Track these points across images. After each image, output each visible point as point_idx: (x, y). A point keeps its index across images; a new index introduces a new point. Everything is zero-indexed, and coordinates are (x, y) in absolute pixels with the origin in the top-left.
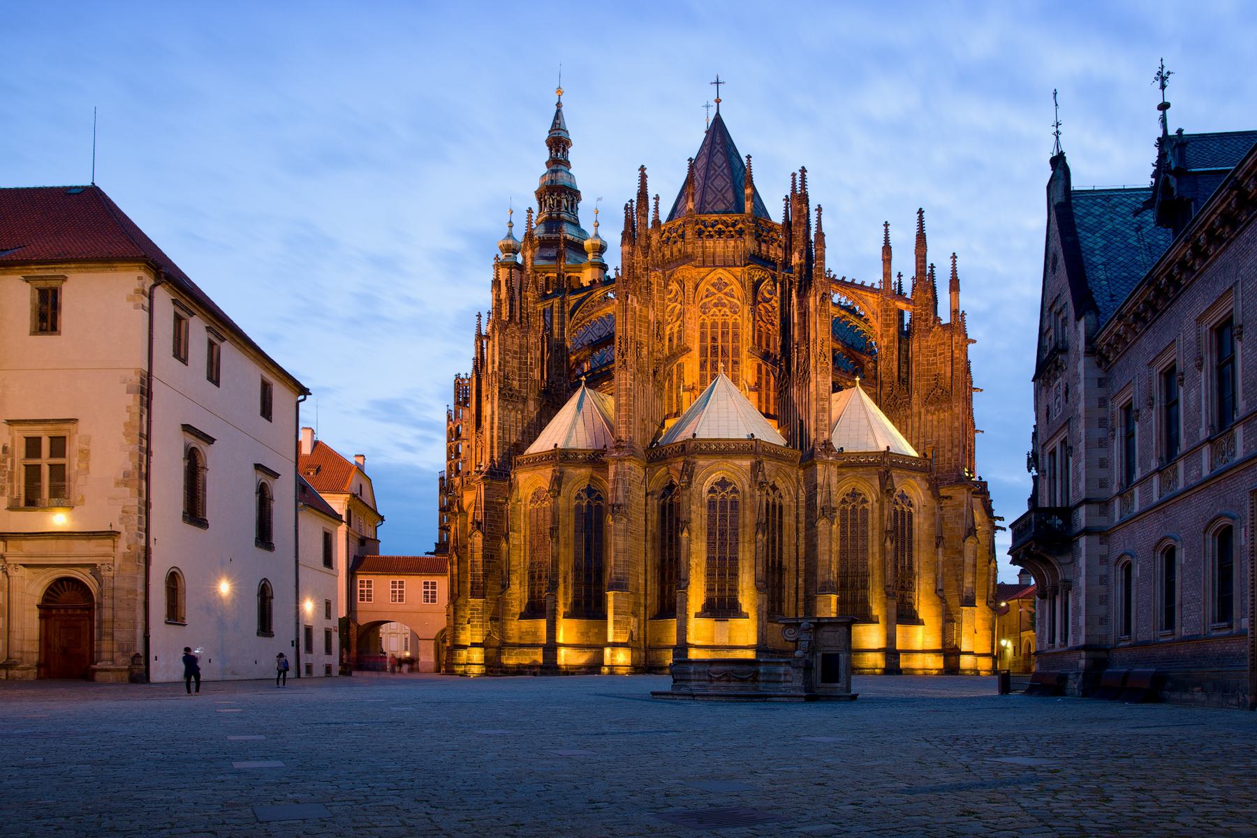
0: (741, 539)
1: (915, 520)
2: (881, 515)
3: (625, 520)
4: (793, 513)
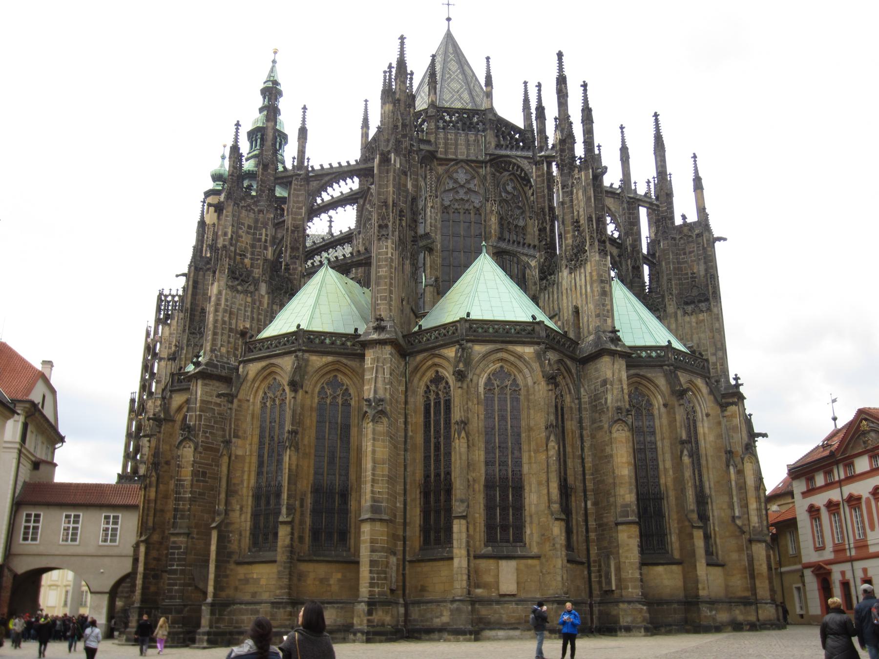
1: (700, 430)
2: (672, 421)
3: (385, 420)
4: (576, 416)
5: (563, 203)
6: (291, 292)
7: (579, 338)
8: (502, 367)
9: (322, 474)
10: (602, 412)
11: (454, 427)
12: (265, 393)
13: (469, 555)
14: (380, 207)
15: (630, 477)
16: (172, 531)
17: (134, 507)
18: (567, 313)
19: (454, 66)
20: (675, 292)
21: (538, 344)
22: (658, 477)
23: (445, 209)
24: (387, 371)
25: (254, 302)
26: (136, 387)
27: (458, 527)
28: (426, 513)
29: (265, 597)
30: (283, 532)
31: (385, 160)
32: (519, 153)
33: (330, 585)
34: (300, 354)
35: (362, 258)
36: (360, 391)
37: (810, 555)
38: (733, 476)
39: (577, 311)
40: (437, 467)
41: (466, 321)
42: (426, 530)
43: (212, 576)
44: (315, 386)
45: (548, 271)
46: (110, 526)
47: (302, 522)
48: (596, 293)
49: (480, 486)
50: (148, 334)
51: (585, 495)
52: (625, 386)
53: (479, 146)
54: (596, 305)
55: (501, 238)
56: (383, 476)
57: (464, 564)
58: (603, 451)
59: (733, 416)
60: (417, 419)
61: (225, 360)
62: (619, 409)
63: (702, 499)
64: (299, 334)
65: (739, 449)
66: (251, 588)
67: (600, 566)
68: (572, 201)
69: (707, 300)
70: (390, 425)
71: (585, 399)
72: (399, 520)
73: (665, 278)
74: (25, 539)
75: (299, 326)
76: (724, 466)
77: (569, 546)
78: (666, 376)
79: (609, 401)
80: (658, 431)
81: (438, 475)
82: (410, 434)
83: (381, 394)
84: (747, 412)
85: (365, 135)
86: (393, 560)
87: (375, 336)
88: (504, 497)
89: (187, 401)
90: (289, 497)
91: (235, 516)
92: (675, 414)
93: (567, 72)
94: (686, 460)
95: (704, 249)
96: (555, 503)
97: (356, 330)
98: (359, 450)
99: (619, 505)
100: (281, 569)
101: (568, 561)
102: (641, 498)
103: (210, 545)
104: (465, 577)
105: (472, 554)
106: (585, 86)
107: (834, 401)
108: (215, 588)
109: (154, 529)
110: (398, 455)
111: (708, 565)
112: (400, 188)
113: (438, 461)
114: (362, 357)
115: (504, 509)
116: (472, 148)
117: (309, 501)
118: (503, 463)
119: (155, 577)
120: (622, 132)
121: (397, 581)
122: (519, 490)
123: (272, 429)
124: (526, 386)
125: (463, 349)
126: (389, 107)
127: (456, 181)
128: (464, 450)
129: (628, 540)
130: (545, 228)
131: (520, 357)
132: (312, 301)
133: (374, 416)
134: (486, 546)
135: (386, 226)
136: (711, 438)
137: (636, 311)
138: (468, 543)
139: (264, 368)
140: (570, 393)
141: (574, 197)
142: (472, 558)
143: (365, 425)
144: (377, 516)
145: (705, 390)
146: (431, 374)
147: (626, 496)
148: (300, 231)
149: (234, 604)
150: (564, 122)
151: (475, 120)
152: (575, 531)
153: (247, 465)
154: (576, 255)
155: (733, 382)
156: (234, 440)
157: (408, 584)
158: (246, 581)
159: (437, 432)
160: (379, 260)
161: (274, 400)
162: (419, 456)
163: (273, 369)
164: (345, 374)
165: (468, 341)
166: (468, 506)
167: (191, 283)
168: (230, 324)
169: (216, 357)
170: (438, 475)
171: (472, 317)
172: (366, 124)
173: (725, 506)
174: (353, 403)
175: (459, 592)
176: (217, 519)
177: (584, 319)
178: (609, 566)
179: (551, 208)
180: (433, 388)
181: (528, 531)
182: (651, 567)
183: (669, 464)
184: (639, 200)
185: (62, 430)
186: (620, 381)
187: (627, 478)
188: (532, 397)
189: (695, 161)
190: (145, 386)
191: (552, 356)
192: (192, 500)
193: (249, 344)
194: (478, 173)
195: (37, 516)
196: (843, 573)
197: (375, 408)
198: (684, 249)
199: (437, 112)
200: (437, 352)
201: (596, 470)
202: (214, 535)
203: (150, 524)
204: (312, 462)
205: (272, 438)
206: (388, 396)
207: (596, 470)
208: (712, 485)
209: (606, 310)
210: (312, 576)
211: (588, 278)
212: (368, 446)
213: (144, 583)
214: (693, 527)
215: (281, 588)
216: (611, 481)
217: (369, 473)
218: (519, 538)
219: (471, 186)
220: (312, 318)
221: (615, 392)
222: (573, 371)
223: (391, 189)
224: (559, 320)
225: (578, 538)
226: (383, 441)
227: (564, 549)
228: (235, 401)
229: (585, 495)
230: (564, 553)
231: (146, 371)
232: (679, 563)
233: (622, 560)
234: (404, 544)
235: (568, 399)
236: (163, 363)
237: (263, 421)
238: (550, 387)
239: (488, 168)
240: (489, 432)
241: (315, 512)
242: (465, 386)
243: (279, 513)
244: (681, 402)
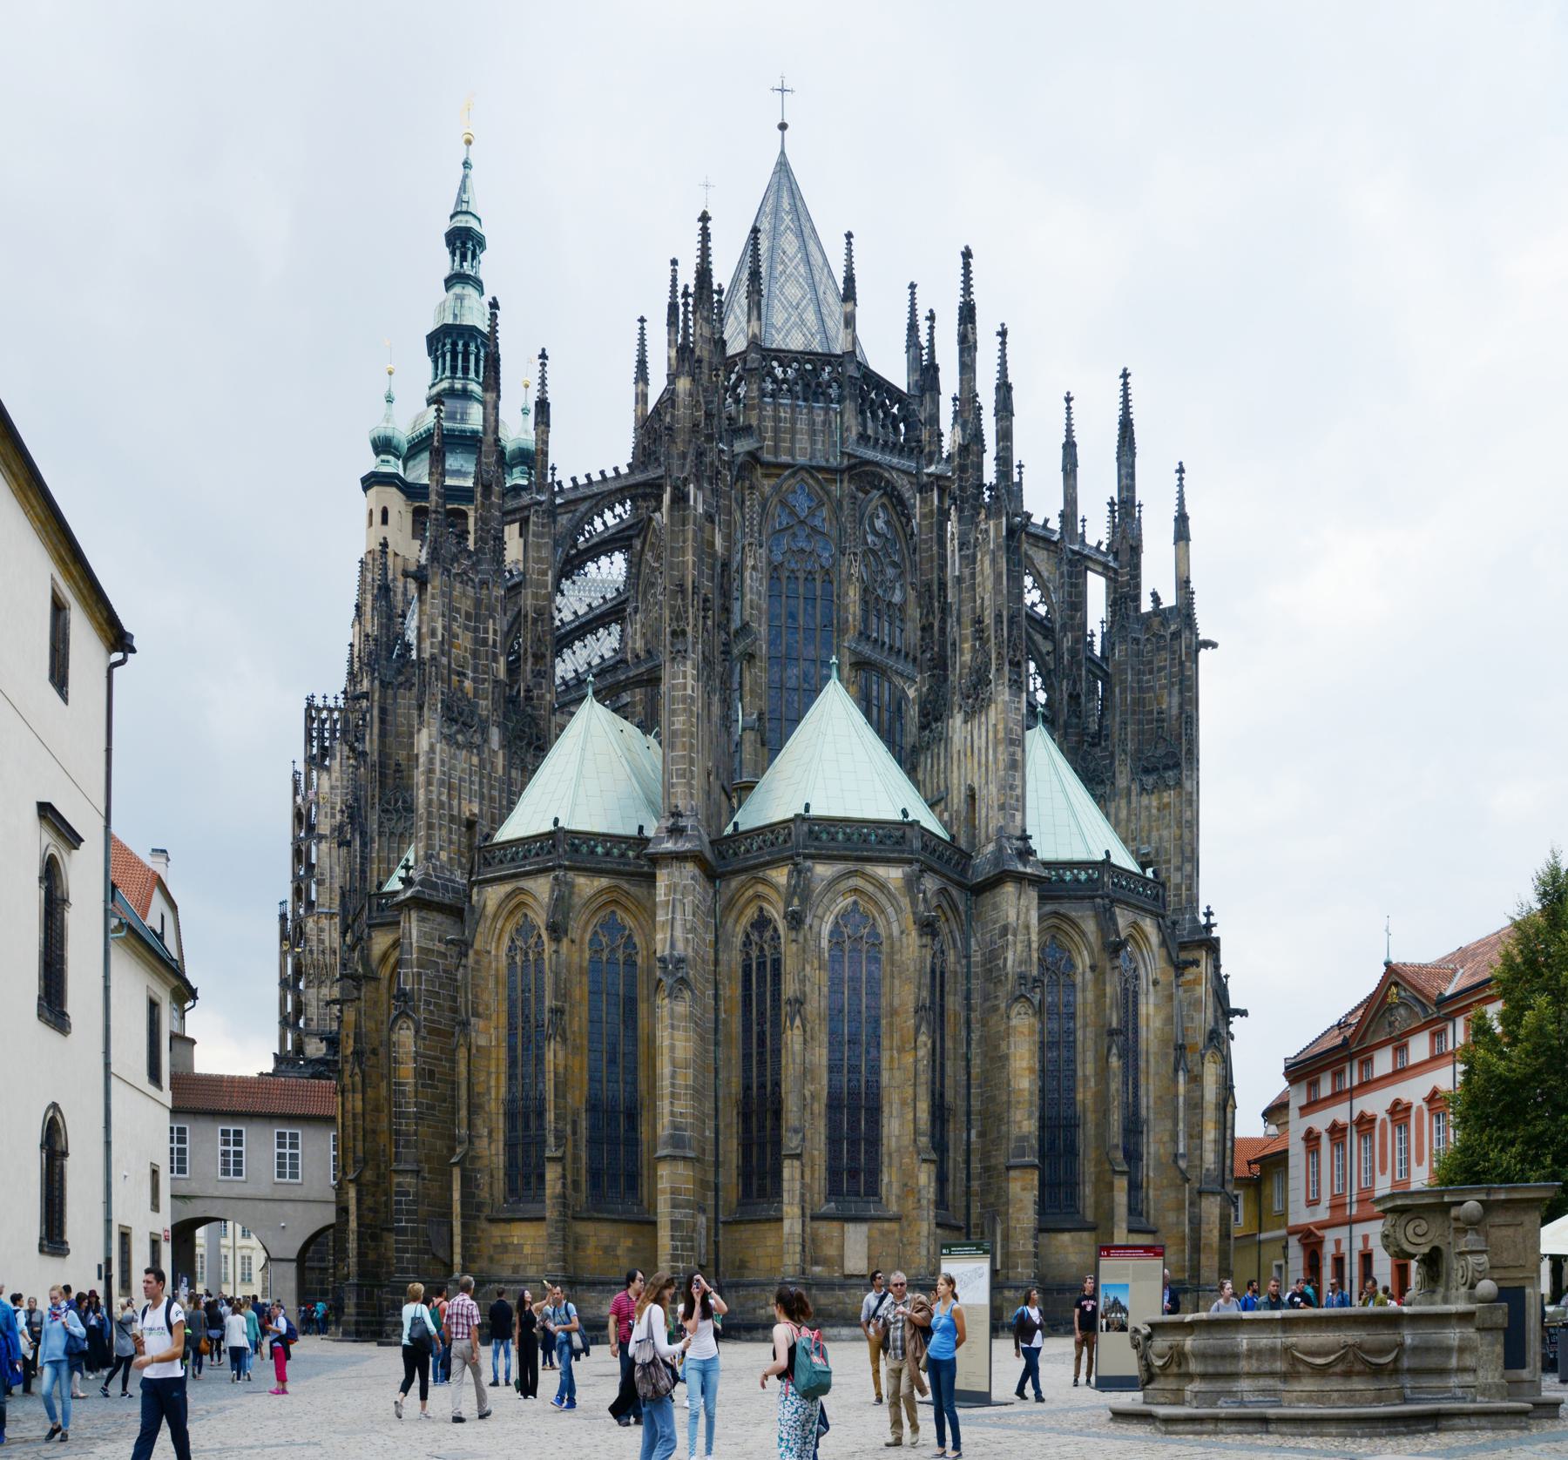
0: (885, 1042)
2: (1100, 996)
9: (600, 1082)
10: (998, 982)
11: (785, 1009)
12: (513, 941)
13: (803, 1215)
14: (674, 594)
15: (1031, 1093)
20: (1130, 747)
23: (775, 569)
24: (688, 909)
30: (552, 1173)
35: (642, 669)
36: (650, 939)
40: (761, 1074)
44: (584, 930)
48: (1001, 765)
53: (831, 434)
54: (1002, 788)
57: (798, 1229)
58: (997, 1047)
70: (694, 999)
75: (556, 821)
77: (941, 1202)
78: (1097, 916)
81: (762, 1086)
82: (723, 1016)
88: (854, 1125)
89: (396, 944)
92: (1104, 983)
96: (924, 1135)
97: (641, 828)
98: (651, 1039)
99: (1013, 1137)
101: (938, 1225)
102: (1046, 1124)
103: (450, 1189)
104: (798, 1248)
105: (808, 1212)
110: (707, 1051)
112: (705, 548)
115: (854, 1143)
117: (583, 1124)
118: (854, 1069)
121: (707, 1253)
122: (875, 1112)
123: (526, 1001)
125: (799, 872)
127: (793, 513)
128: (798, 1047)
130: (931, 625)
133: (671, 988)
137: (1064, 791)
138: (803, 1200)
140: (955, 946)
143: (659, 1002)
144: (679, 1152)
148: (544, 614)
149: (490, 1282)
153: (493, 1062)
160: (673, 700)
161: (526, 954)
162: (736, 1053)
163: (522, 897)
164: (626, 909)
169: (434, 869)
170: (762, 1086)
171: (813, 812)
172: (642, 365)
175: (790, 1270)
179: (943, 586)
184: (1087, 557)
188: (897, 957)
191: (930, 884)
193: (484, 856)
194: (828, 493)
197: (673, 974)
198: (1150, 662)
199: (763, 355)
207: (986, 1080)
209: (1014, 801)
211: (991, 735)
212: (664, 1037)
216: (1005, 1098)
217: (667, 1082)
219: (817, 522)
224: (946, 809)
233: (1012, 1223)
238: (925, 940)
240: (835, 1014)
242: (801, 939)
243: (542, 1143)
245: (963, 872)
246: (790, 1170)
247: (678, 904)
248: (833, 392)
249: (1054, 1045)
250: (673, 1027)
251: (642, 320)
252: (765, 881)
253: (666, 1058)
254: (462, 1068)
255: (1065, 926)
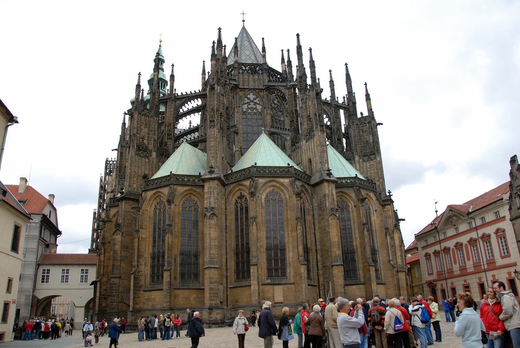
1: (372, 218)
2: (359, 214)
3: (215, 218)
4: (311, 213)
5: (301, 108)
6: (168, 156)
7: (312, 174)
8: (273, 189)
13: (259, 284)
15: (338, 243)
16: (112, 276)
17: (95, 265)
18: (305, 162)
19: (246, 43)
20: (358, 151)
21: (291, 177)
22: (352, 242)
25: (149, 162)
26: (96, 206)
27: (253, 270)
28: (237, 264)
29: (158, 307)
30: (166, 275)
31: (212, 88)
32: (279, 84)
33: (190, 301)
34: (172, 186)
36: (203, 204)
37: (426, 278)
38: (389, 240)
39: (310, 161)
41: (255, 167)
42: (237, 273)
43: (132, 298)
45: (295, 142)
46: (84, 274)
47: (175, 270)
49: (263, 249)
50: (101, 180)
51: (317, 252)
52: (335, 197)
55: (272, 127)
56: (215, 245)
57: (257, 288)
58: (325, 230)
59: (388, 210)
60: (232, 217)
61: (136, 190)
62: (332, 209)
63: (374, 252)
64: (171, 175)
65: (391, 227)
66: (151, 303)
67: (324, 287)
68: (306, 106)
69: (374, 154)
71: (315, 204)
72: (224, 267)
73: (354, 144)
74: (43, 282)
76: (384, 235)
77: (309, 278)
79: (327, 205)
80: (352, 219)
81: (243, 244)
82: (228, 224)
83: (213, 205)
84: (395, 209)
85: (204, 78)
86: (221, 287)
87: (209, 176)
89: (118, 212)
90: (168, 257)
91: (142, 268)
93: (302, 44)
94: (366, 233)
95: (372, 129)
97: (200, 173)
98: (203, 233)
99: (333, 256)
100: (165, 293)
104: (257, 295)
106: (310, 50)
107: (436, 203)
108: (134, 303)
109: (104, 275)
110: (223, 235)
111: (377, 284)
113: (242, 237)
114: (203, 186)
115: (276, 260)
116: (257, 82)
119: (105, 298)
120: (330, 73)
122: (283, 250)
123: (159, 223)
124: (286, 198)
125: (254, 181)
126: (214, 62)
127: (249, 99)
128: (255, 231)
129: (338, 273)
131: (282, 184)
132: (178, 160)
134: (267, 279)
135: (214, 121)
136: (378, 222)
138: (258, 277)
139: (154, 194)
141: (307, 104)
142: (260, 285)
143: (205, 220)
145: (374, 198)
146: (238, 194)
147: (337, 252)
150: (301, 66)
151: (258, 69)
152: (312, 270)
153: (147, 242)
154: (309, 133)
155: (388, 194)
156: (141, 230)
157: (229, 299)
158: (149, 300)
159: (242, 223)
162: (233, 235)
165: (256, 177)
166: (258, 259)
167: (119, 153)
168: (138, 173)
170: (243, 244)
171: (258, 165)
173: (385, 255)
174: (199, 210)
176: (133, 269)
177: (314, 165)
178: (329, 287)
179: (296, 111)
180: (239, 201)
181: (288, 271)
182: (349, 286)
183: (357, 235)
185: (60, 228)
186: (332, 195)
187: (337, 243)
189: (366, 86)
190: (100, 206)
191: (299, 183)
192: (121, 260)
193: (148, 182)
195: (49, 270)
196: (442, 285)
199: (239, 65)
200: (241, 183)
201: (322, 240)
202: (132, 276)
203: (102, 273)
204: (180, 240)
205: (160, 229)
206: (216, 206)
208: (379, 244)
209: (324, 160)
210: (181, 296)
212: (207, 231)
213: (99, 301)
214: (370, 266)
215: (166, 302)
216: (329, 244)
217: (208, 244)
218: (284, 274)
220: (178, 168)
221: (330, 201)
222: (309, 191)
223: (216, 103)
225: (314, 274)
226: (215, 228)
227: (306, 279)
228: (141, 210)
229: (317, 252)
230: (306, 281)
231: (101, 199)
232: (364, 284)
233: (335, 283)
234: (227, 279)
235: (307, 205)
236: (109, 195)
237: (155, 220)
239: (265, 92)
240: (268, 222)
241: (181, 264)
244: (363, 204)
245: (309, 181)
246: (253, 270)
247: (212, 192)
248: (260, 72)
249: (344, 229)
250: (210, 228)
251: (204, 61)
252: (242, 185)
253: (208, 237)
254: (136, 244)
255: (344, 195)
